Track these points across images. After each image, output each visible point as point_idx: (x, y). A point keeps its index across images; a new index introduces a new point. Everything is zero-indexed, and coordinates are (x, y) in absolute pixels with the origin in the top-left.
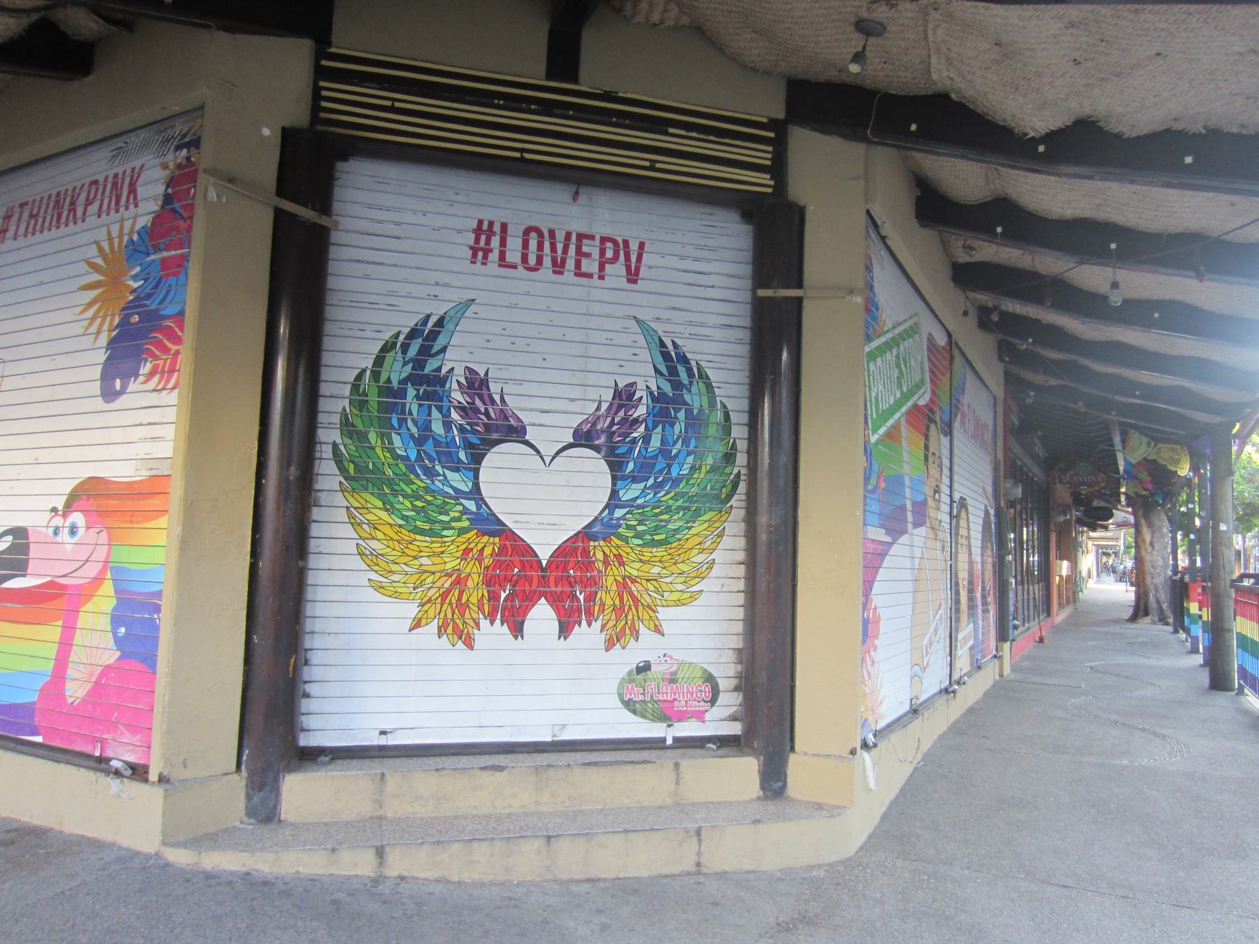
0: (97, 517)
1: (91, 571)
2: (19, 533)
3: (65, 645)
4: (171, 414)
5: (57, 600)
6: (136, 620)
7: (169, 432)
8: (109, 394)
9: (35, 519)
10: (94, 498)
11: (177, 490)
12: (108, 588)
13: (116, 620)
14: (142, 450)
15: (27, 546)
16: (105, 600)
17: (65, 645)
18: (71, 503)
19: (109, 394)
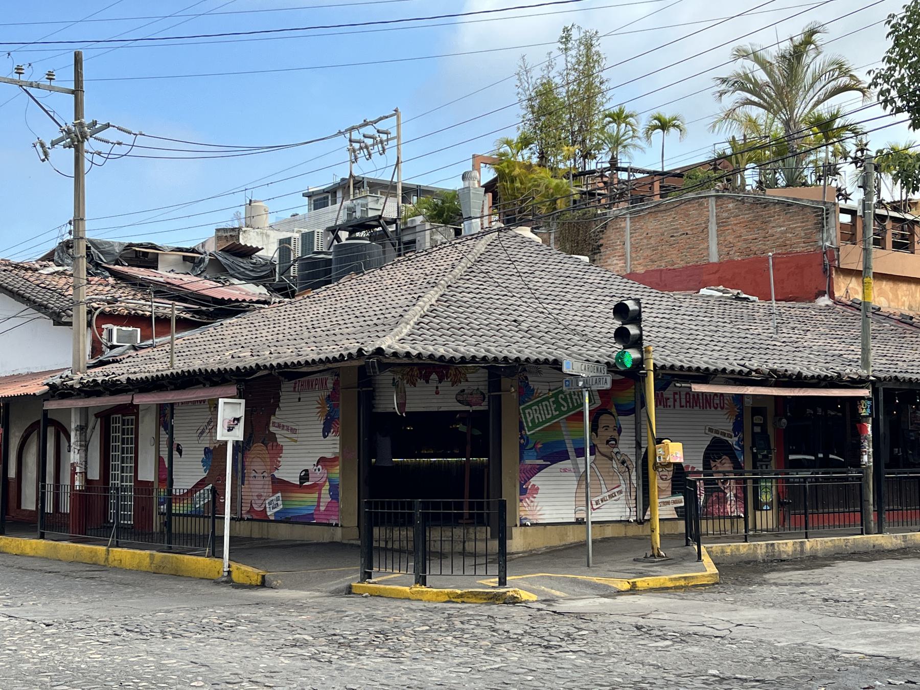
0: (324, 466)
1: (324, 479)
2: (306, 471)
3: (319, 498)
4: (338, 442)
5: (316, 487)
6: (334, 490)
7: (338, 446)
8: (325, 437)
9: (310, 468)
10: (322, 461)
11: (341, 459)
12: (327, 483)
13: (330, 490)
14: (332, 450)
15: (308, 475)
16: (327, 487)
17: (319, 498)
18: (318, 462)
19: (325, 437)
